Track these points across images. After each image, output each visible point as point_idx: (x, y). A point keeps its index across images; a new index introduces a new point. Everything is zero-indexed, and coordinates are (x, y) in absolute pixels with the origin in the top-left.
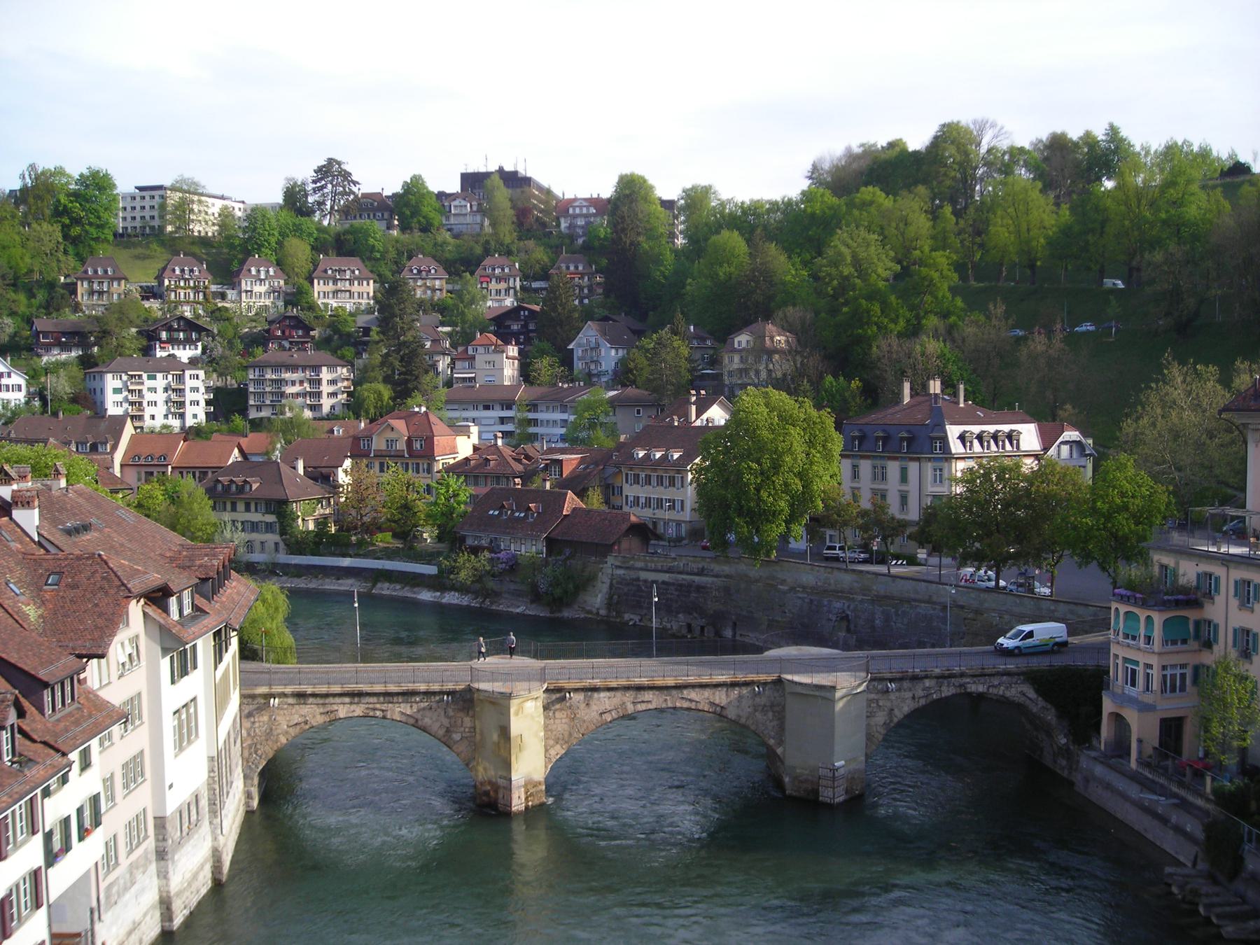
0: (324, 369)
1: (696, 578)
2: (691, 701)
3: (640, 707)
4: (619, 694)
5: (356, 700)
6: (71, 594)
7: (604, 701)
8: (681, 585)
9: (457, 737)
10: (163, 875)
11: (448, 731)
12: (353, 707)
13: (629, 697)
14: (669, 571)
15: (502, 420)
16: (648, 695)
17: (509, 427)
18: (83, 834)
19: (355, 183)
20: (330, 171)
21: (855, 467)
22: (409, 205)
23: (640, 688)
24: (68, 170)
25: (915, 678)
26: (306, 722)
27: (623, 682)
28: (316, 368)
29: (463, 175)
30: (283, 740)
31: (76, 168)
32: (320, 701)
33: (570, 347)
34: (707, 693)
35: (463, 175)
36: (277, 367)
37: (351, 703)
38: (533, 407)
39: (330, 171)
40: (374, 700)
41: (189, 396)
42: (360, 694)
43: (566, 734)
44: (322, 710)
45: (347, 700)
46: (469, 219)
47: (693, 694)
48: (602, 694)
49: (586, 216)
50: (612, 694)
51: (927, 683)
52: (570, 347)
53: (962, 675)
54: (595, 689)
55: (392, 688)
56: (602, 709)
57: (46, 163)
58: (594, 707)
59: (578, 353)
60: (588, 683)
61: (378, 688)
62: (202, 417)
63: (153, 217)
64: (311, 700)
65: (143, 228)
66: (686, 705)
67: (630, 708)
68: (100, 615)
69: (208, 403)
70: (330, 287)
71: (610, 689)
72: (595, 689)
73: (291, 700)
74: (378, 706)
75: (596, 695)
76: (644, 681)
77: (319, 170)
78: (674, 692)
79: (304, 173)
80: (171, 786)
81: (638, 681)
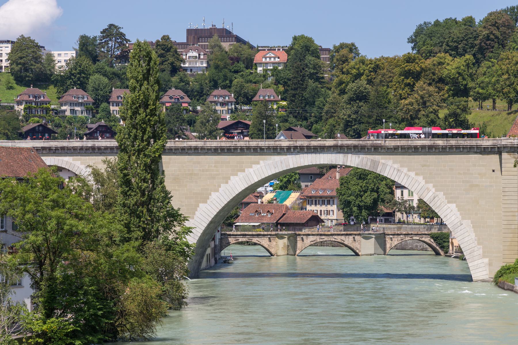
3: (321, 240)
13: (318, 237)
16: (323, 237)
20: (112, 32)
21: (402, 192)
23: (321, 235)
25: (398, 235)
34: (339, 237)
39: (112, 32)
46: (198, 65)
47: (336, 237)
49: (273, 63)
51: (402, 236)
53: (412, 234)
54: (309, 235)
66: (334, 240)
67: (318, 240)
71: (313, 235)
72: (309, 235)
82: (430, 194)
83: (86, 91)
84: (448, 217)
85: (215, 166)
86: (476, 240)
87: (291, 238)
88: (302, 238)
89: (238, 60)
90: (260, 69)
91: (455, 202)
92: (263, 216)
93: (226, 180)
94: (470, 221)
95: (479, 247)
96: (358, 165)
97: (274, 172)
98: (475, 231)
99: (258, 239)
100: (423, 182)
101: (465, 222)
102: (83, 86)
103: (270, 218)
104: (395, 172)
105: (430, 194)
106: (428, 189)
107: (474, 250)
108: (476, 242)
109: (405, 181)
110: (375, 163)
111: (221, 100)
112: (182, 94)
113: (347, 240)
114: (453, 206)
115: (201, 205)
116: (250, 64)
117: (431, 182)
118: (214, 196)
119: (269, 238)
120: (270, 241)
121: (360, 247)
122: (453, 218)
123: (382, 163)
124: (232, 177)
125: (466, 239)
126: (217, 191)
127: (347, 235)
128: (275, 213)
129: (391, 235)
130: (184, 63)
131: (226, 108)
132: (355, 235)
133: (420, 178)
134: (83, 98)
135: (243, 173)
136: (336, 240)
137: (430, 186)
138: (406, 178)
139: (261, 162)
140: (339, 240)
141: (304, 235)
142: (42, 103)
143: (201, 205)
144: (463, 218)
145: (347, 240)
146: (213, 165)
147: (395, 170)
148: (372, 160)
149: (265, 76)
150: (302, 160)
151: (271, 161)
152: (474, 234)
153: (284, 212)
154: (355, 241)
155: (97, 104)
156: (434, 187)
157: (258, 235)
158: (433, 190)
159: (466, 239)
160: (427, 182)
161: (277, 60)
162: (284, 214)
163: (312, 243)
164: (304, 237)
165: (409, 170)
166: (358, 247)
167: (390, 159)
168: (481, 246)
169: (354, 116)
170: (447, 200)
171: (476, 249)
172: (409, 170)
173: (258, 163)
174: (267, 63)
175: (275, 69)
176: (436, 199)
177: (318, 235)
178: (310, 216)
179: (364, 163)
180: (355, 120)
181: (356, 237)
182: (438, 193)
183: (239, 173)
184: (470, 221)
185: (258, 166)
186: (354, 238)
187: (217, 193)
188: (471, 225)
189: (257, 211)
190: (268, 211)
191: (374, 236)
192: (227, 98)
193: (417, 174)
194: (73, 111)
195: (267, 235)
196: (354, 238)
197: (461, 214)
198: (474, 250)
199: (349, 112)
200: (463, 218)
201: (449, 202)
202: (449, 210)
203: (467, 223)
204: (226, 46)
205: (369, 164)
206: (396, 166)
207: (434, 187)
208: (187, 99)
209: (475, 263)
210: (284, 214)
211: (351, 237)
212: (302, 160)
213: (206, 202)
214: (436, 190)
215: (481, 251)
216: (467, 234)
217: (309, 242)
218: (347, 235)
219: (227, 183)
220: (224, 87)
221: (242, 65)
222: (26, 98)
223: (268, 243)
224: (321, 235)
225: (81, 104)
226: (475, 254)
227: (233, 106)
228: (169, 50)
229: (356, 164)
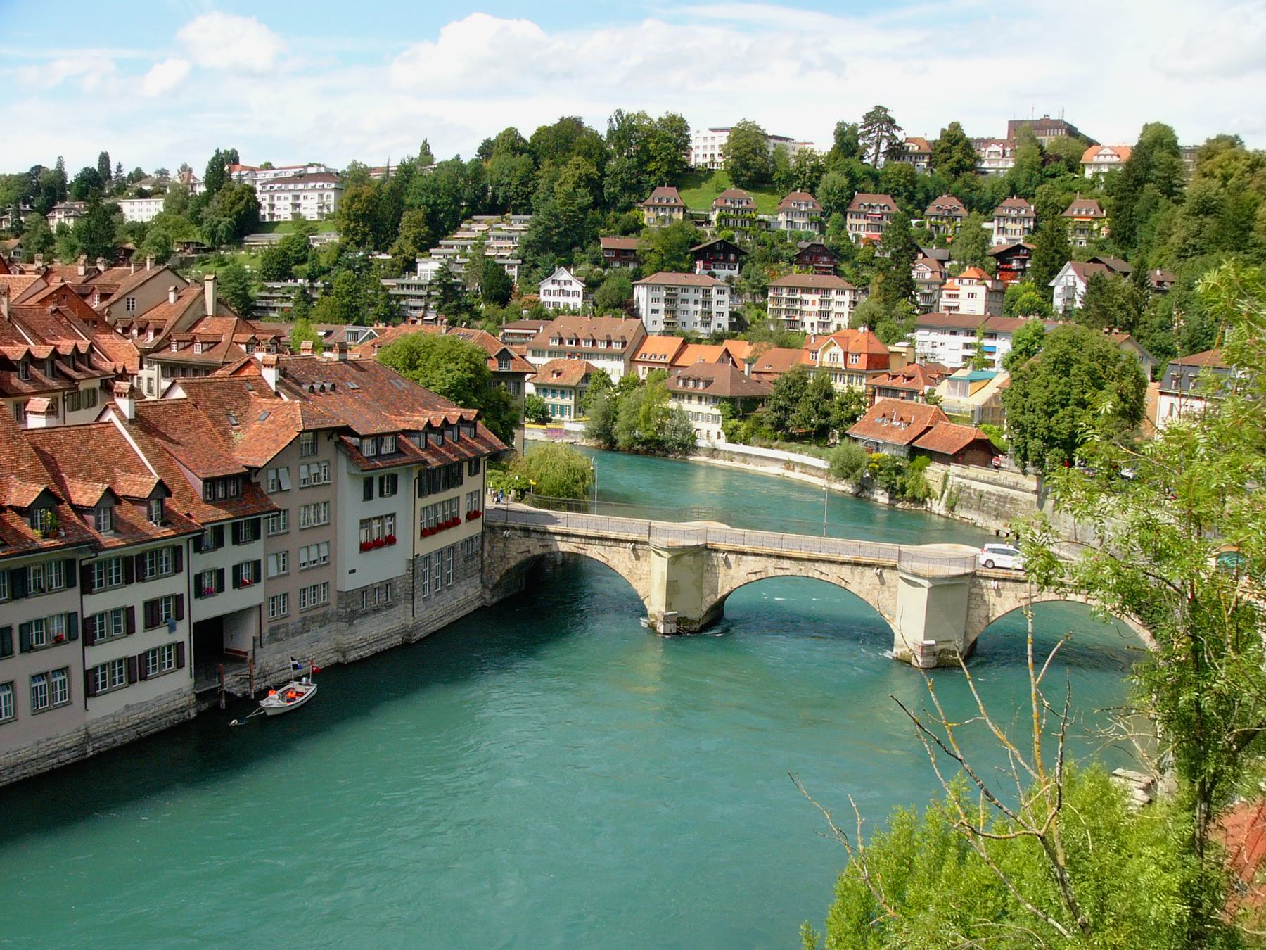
0: (834, 292)
1: (1012, 492)
3: (780, 573)
4: (763, 559)
7: (751, 563)
8: (1000, 496)
14: (993, 483)
15: (967, 346)
16: (786, 564)
17: (969, 352)
18: (238, 583)
19: (899, 129)
20: (880, 119)
22: (956, 151)
23: (779, 557)
24: (649, 115)
27: (767, 550)
28: (827, 291)
29: (1011, 122)
30: (513, 563)
31: (656, 112)
32: (539, 536)
33: (1051, 284)
34: (835, 568)
35: (1011, 122)
36: (792, 289)
38: (993, 336)
39: (880, 119)
40: (578, 540)
41: (715, 308)
42: (568, 535)
47: (824, 567)
48: (750, 558)
49: (1109, 164)
50: (758, 558)
52: (1051, 284)
55: (591, 533)
57: (630, 109)
58: (742, 567)
59: (1058, 290)
60: (739, 547)
61: (582, 532)
62: (726, 325)
64: (533, 535)
66: (817, 575)
67: (771, 573)
69: (732, 314)
70: (863, 222)
73: (519, 533)
75: (744, 557)
76: (784, 552)
77: (868, 116)
79: (855, 118)
80: (352, 571)
81: (778, 551)
83: (814, 196)
87: (687, 559)
89: (1058, 158)
90: (1088, 173)
92: (893, 427)
102: (812, 191)
103: (903, 432)
111: (1014, 213)
112: (955, 202)
116: (1074, 166)
120: (637, 558)
129: (995, 579)
130: (983, 162)
131: (1020, 227)
134: (806, 205)
136: (823, 577)
140: (833, 578)
141: (730, 552)
142: (744, 210)
149: (1094, 183)
154: (883, 583)
155: (826, 213)
157: (602, 539)
161: (1115, 159)
162: (929, 428)
163: (754, 578)
164: (731, 557)
169: (1191, 241)
174: (1099, 164)
175: (1109, 175)
177: (770, 556)
178: (969, 440)
180: (1194, 247)
191: (926, 583)
192: (1023, 212)
194: (790, 223)
195: (626, 541)
196: (880, 576)
199: (1183, 233)
204: (1048, 140)
208: (963, 211)
210: (929, 428)
211: (870, 573)
217: (743, 573)
220: (1026, 197)
221: (1062, 166)
222: (721, 203)
224: (779, 557)
225: (802, 214)
227: (1032, 223)
228: (957, 142)
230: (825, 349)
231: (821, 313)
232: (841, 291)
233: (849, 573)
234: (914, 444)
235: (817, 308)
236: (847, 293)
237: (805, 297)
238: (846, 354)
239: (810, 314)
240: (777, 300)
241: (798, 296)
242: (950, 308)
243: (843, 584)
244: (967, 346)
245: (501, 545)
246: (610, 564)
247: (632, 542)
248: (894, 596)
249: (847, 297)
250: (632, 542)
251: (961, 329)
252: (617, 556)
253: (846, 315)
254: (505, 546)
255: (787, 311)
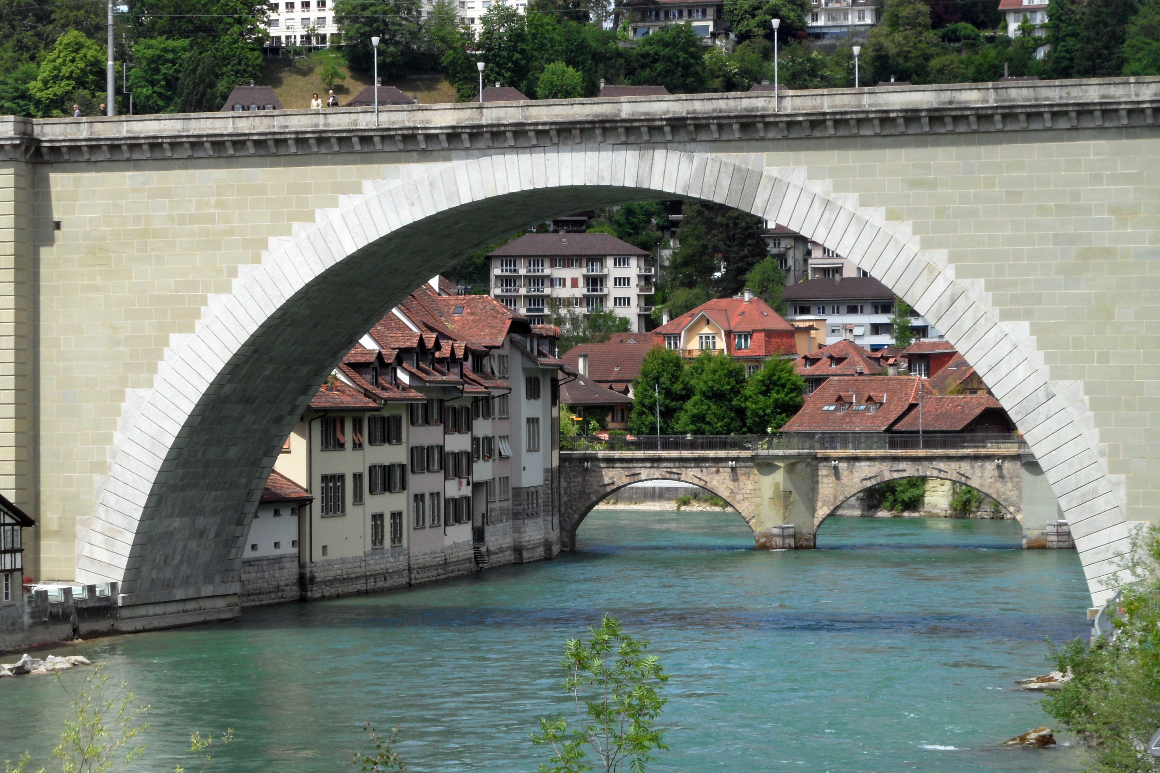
0: (610, 262)
2: (940, 471)
5: (656, 465)
6: (471, 318)
9: (739, 497)
10: (517, 530)
11: (732, 492)
12: (653, 471)
15: (876, 329)
16: (902, 465)
26: (613, 483)
32: (625, 465)
34: (954, 465)
36: (535, 260)
37: (651, 467)
43: (832, 496)
44: (627, 473)
45: (649, 465)
46: (852, 19)
47: (942, 465)
56: (863, 476)
58: (856, 474)
63: (321, 21)
64: (617, 465)
65: (307, 38)
67: (887, 476)
68: (492, 327)
74: (674, 470)
75: (857, 464)
78: (926, 463)
82: (940, 285)
84: (1003, 368)
85: (219, 204)
86: (1102, 454)
87: (801, 466)
88: (835, 468)
90: (1013, 28)
91: (1027, 315)
92: (857, 412)
93: (255, 249)
94: (1080, 383)
95: (1114, 477)
96: (688, 186)
97: (408, 220)
98: (1099, 422)
99: (696, 472)
100: (913, 246)
101: (1061, 387)
103: (874, 417)
104: (817, 209)
105: (940, 285)
106: (929, 267)
107: (1095, 490)
108: (1103, 462)
109: (849, 239)
110: (746, 179)
113: (978, 473)
114: (1020, 330)
115: (174, 338)
117: (941, 245)
118: (216, 304)
119: (733, 469)
121: (1019, 496)
122: (1020, 374)
123: (770, 178)
124: (272, 241)
125: (1068, 451)
126: (225, 288)
127: (976, 458)
128: (889, 401)
132: (1004, 458)
133: (903, 231)
135: (308, 224)
137: (939, 256)
138: (853, 229)
139: (367, 185)
143: (174, 338)
144: (1056, 375)
145: (978, 473)
146: (213, 200)
147: (817, 204)
148: (736, 169)
150: (500, 175)
151: (399, 182)
152: (1096, 432)
153: (911, 401)
154: (1001, 476)
156: (952, 259)
158: (950, 272)
159: (1068, 451)
160: (926, 244)
162: (912, 407)
164: (843, 466)
165: (864, 203)
166: (1013, 495)
167: (797, 163)
168: (1123, 477)
170: (997, 310)
171: (1103, 486)
172: (864, 203)
173: (356, 189)
176: (961, 304)
178: (978, 411)
179: (710, 179)
181: (1007, 466)
182: (965, 283)
183: (296, 226)
184: (1080, 383)
185: (357, 200)
186: (999, 467)
187: (225, 298)
188: (1086, 398)
189: (839, 399)
190: (870, 399)
193: (891, 216)
195: (727, 459)
197: (1048, 359)
198: (1095, 490)
200: (1056, 375)
201: (1005, 316)
202: (1005, 347)
203: (1070, 391)
205: (725, 182)
206: (820, 187)
207: (952, 259)
209: (1102, 538)
210: (912, 407)
211: (990, 467)
212: (500, 175)
213: (190, 329)
214: (961, 274)
215: (1121, 495)
216: (1069, 432)
217: (857, 480)
218: (976, 458)
219: (257, 260)
223: (731, 484)
226: (1101, 504)
229: (681, 183)
230: (691, 331)
231: (587, 300)
232: (621, 260)
233: (969, 468)
234: (896, 428)
235: (581, 291)
236: (633, 262)
237: (559, 273)
238: (728, 334)
239: (568, 302)
240: (506, 281)
241: (547, 271)
242: (825, 271)
243: (963, 480)
244: (876, 329)
245: (580, 479)
246: (709, 486)
247: (732, 459)
248: (1018, 487)
249: (633, 269)
250: (732, 459)
251: (864, 300)
252: (716, 477)
253: (634, 301)
254: (584, 479)
255: (529, 299)
